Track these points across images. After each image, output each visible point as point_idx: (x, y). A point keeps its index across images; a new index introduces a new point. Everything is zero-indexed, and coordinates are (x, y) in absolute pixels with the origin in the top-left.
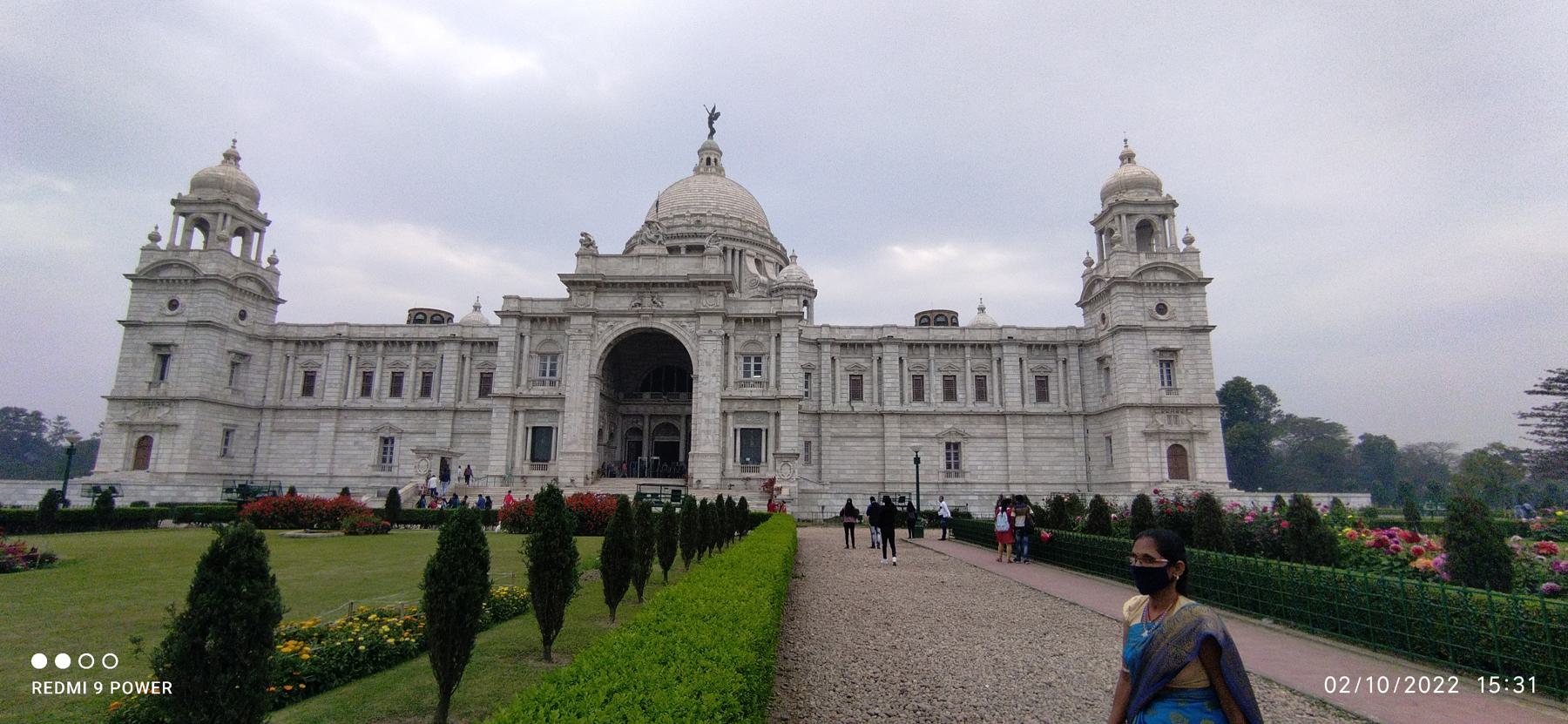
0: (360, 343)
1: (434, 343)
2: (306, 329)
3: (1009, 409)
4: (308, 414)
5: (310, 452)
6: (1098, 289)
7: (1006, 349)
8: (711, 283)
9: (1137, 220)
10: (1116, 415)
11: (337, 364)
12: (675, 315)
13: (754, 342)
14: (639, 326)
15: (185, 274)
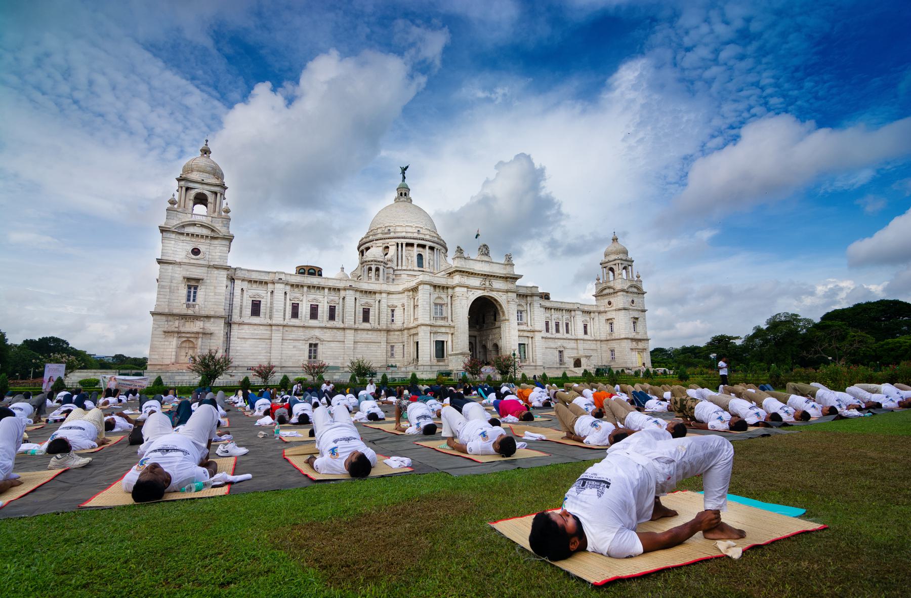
0: (292, 285)
1: (339, 290)
2: (253, 273)
3: (579, 337)
4: (261, 327)
5: (264, 351)
6: (607, 291)
7: (577, 312)
8: (514, 278)
9: (623, 266)
10: (619, 341)
11: (280, 297)
12: (498, 291)
13: (519, 305)
14: (484, 294)
15: (205, 232)
